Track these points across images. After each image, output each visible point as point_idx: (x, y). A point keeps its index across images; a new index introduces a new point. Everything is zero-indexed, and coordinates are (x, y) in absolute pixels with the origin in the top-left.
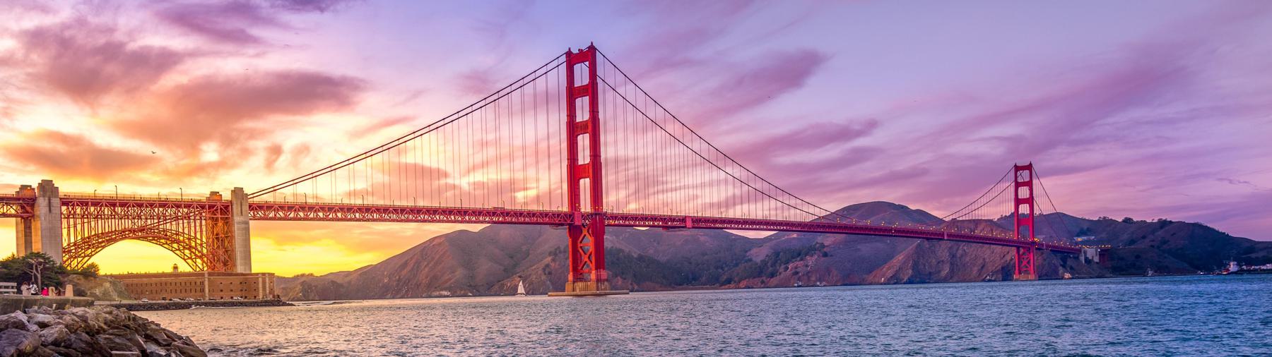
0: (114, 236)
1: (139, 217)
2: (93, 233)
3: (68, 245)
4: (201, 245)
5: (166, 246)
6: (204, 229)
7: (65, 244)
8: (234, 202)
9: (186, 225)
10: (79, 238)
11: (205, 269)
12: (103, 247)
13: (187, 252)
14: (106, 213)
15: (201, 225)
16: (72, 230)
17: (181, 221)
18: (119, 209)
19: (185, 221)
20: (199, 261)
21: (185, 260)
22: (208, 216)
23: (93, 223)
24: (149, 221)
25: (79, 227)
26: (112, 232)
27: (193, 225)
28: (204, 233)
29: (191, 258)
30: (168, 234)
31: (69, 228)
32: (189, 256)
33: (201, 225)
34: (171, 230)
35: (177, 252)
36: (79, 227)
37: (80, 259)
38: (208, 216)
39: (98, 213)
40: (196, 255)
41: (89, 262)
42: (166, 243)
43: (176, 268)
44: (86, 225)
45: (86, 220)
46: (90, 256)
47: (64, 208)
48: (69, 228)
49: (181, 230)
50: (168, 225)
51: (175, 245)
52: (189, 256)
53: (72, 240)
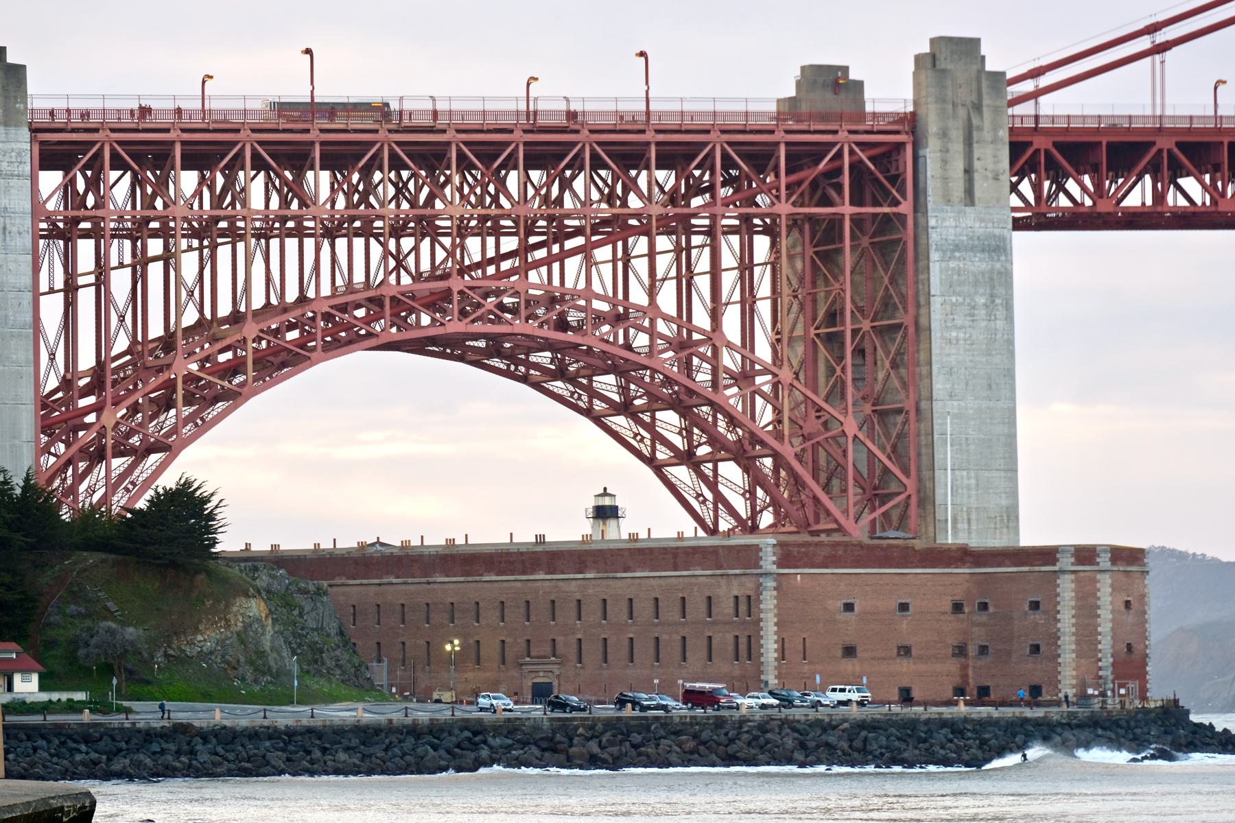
0: (293, 335)
1: (426, 227)
2: (190, 317)
3: (66, 383)
4: (744, 378)
5: (558, 386)
6: (764, 289)
7: (53, 383)
8: (932, 126)
9: (664, 263)
10: (121, 343)
11: (766, 519)
12: (236, 397)
13: (669, 420)
14: (257, 199)
15: (746, 266)
16: (86, 298)
17: (640, 245)
18: (320, 182)
19: (663, 242)
20: (730, 471)
21: (658, 468)
22: (785, 208)
23: (189, 264)
24: (473, 244)
25: (120, 282)
26: (285, 308)
27: (703, 263)
28: (764, 309)
29: (687, 458)
30: (573, 317)
31: (71, 289)
32: (678, 442)
33: (746, 266)
34: (589, 294)
35: (620, 422)
36: (120, 282)
37: (119, 464)
38: (785, 208)
39: (217, 201)
40: (715, 440)
41: (168, 480)
42: (561, 373)
43: (605, 513)
44: (155, 271)
45: (155, 247)
46: (168, 447)
47: (51, 180)
48: (71, 289)
49: (638, 296)
50: (573, 264)
51: (607, 383)
52: (678, 442)
53: (86, 359)
